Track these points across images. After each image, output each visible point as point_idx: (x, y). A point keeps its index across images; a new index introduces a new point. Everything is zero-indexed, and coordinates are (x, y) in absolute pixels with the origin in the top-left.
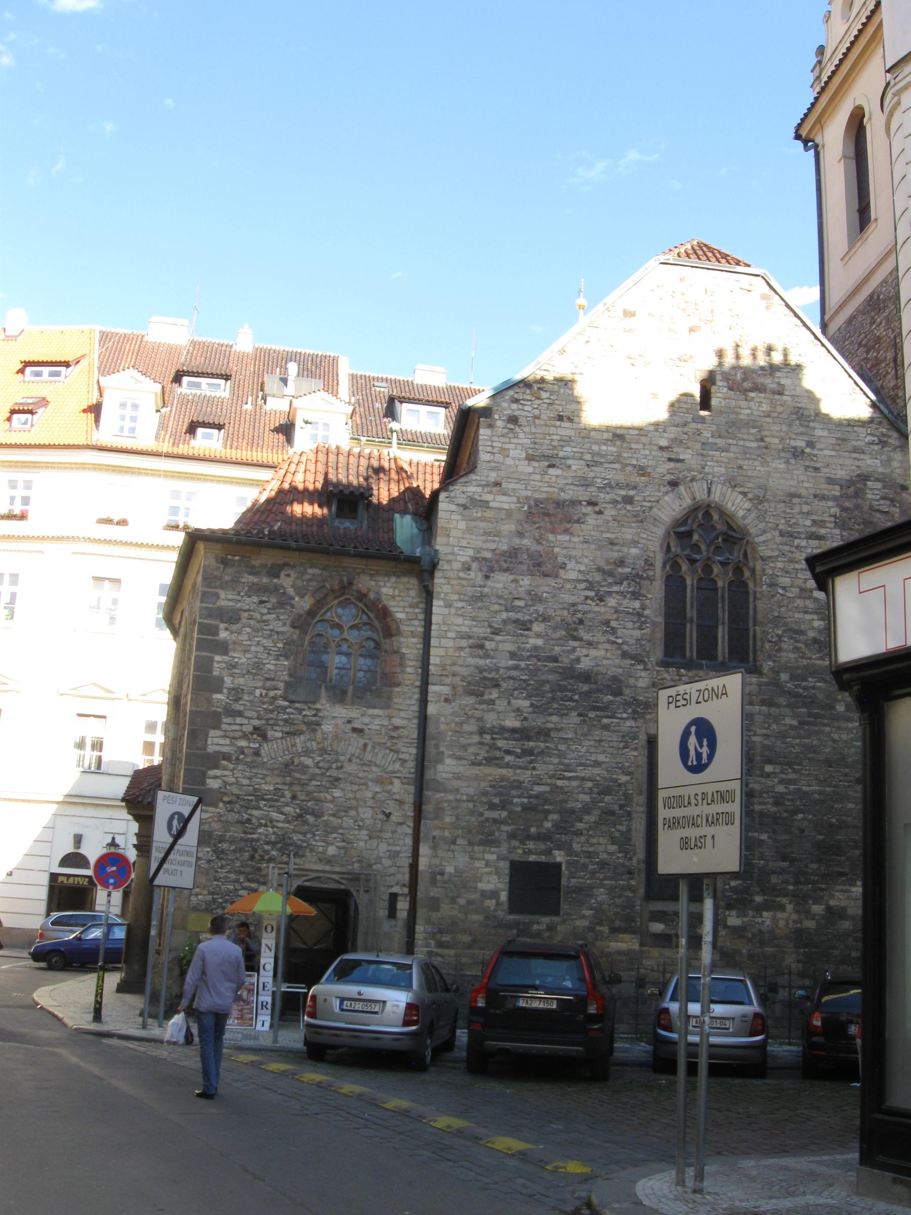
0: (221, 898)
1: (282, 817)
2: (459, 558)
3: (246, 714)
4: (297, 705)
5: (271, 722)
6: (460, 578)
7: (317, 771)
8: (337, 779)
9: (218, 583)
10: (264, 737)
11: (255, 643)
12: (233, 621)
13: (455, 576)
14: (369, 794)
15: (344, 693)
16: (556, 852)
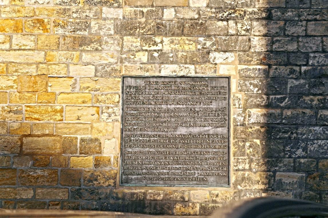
16: (217, 57)
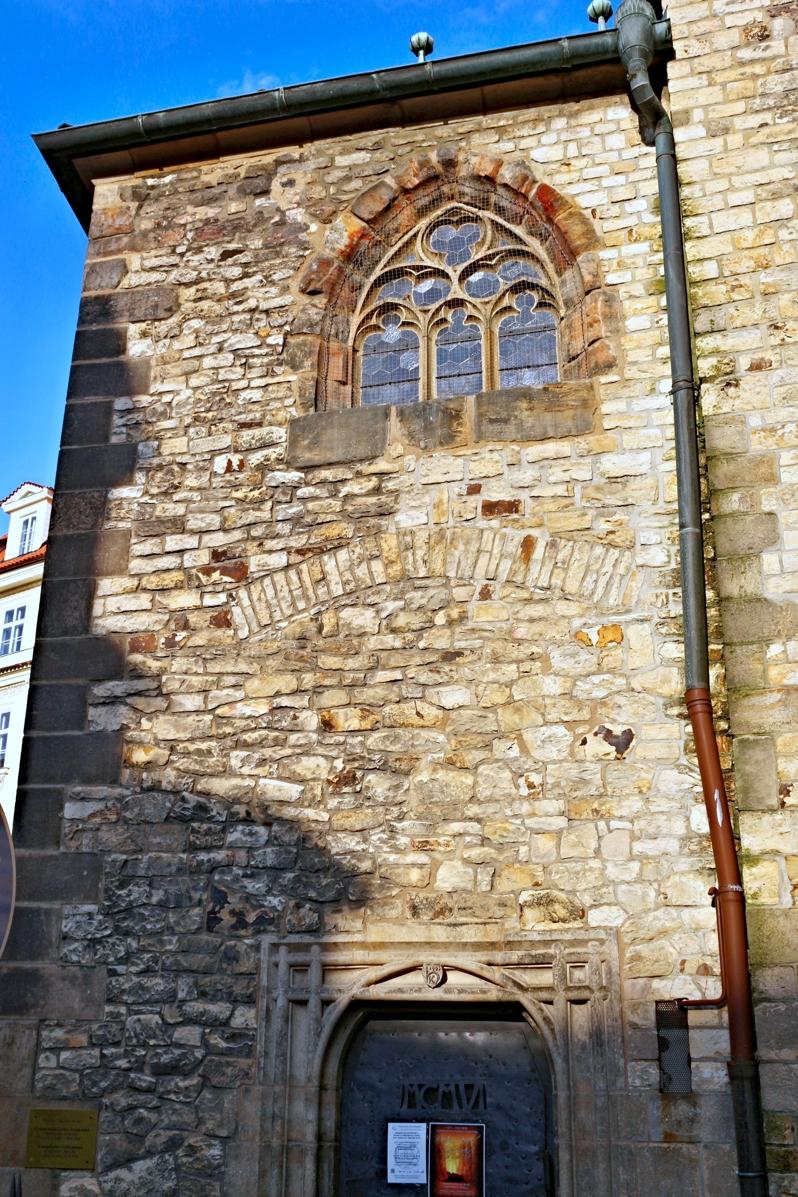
0: (126, 1054)
1: (293, 791)
2: (729, 21)
3: (193, 523)
4: (327, 474)
5: (257, 532)
6: (742, 64)
7: (391, 641)
8: (451, 656)
9: (125, 240)
10: (241, 573)
11: (213, 349)
12: (161, 313)
13: (728, 62)
14: (552, 686)
15: (453, 416)
